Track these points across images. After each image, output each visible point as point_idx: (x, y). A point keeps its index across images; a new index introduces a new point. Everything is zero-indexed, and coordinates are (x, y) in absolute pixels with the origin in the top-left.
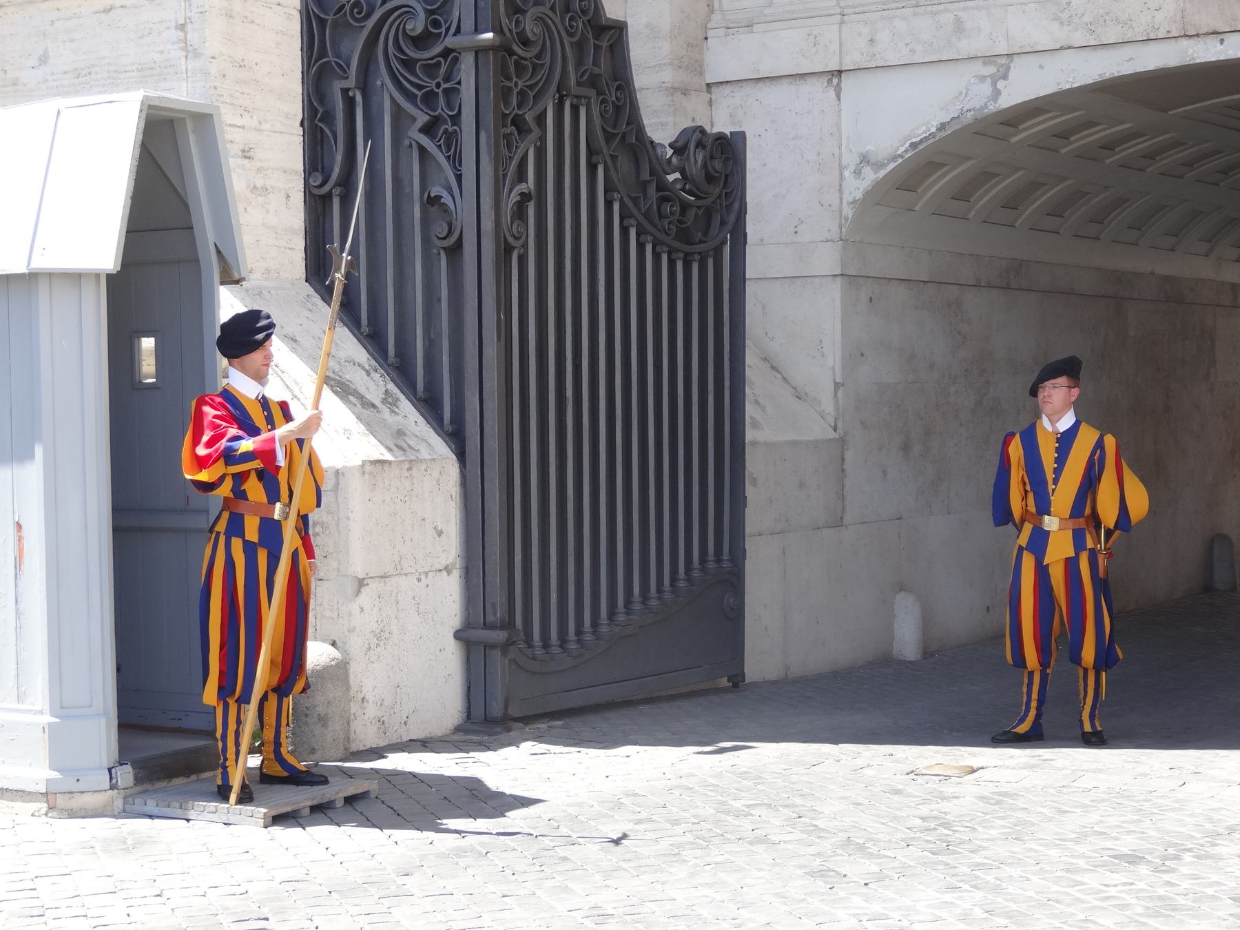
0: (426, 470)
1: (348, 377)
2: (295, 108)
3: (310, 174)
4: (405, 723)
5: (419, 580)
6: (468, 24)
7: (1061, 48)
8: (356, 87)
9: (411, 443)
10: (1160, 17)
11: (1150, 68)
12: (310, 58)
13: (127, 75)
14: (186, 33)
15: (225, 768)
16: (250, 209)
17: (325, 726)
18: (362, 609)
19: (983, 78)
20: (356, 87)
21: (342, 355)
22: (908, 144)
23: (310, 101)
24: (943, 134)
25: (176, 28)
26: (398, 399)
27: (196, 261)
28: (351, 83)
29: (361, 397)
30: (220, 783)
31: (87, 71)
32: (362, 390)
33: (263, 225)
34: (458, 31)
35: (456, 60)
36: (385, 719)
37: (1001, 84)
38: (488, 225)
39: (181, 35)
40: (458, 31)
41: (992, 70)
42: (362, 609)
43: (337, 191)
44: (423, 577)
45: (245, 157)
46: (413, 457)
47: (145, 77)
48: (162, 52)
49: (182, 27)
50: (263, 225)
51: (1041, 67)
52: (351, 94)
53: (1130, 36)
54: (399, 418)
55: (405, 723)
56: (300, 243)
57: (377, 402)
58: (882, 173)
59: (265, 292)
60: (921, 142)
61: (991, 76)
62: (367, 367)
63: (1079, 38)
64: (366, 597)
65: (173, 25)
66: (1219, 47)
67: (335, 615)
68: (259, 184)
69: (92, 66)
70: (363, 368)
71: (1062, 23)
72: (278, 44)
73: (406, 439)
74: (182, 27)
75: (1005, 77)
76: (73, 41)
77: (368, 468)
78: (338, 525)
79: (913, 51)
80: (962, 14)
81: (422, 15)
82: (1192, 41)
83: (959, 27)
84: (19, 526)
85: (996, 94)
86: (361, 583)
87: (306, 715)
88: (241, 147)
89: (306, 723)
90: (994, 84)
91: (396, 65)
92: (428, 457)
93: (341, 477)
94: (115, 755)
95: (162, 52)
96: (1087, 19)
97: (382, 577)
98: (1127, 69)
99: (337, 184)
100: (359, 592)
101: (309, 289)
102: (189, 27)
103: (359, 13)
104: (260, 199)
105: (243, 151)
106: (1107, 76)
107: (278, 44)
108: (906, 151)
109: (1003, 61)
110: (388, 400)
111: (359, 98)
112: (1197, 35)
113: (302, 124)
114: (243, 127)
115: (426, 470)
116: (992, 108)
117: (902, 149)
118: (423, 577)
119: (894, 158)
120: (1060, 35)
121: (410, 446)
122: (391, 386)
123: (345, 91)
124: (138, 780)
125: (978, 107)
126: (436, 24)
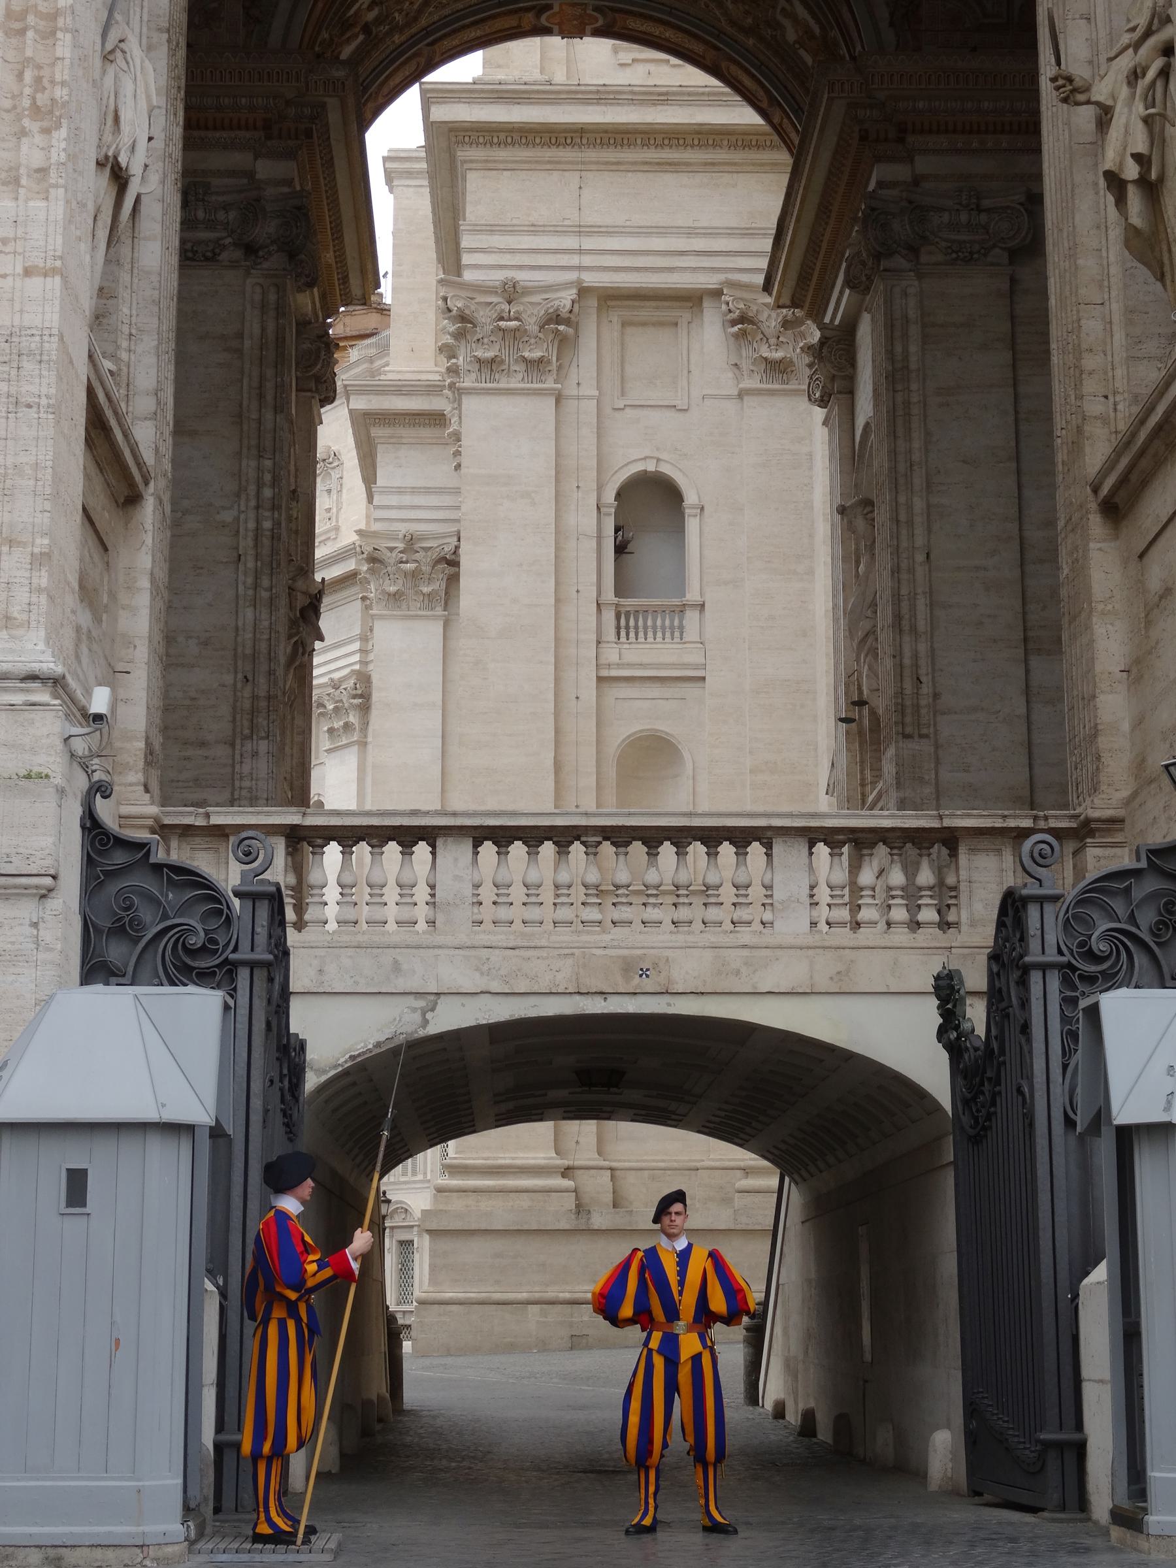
6: (245, 944)
7: (482, 992)
10: (560, 976)
11: (550, 1014)
19: (414, 1010)
22: (347, 1056)
24: (379, 1051)
25: (31, 925)
34: (235, 950)
35: (230, 972)
37: (429, 1016)
38: (257, 1103)
39: (35, 932)
40: (235, 950)
41: (421, 1003)
48: (13, 943)
49: (35, 925)
51: (463, 1005)
53: (536, 989)
58: (324, 1078)
60: (359, 1055)
61: (422, 1009)
63: (496, 986)
65: (27, 922)
66: (603, 1003)
71: (482, 974)
74: (35, 925)
75: (433, 1010)
79: (356, 983)
80: (399, 958)
81: (202, 934)
82: (582, 997)
83: (397, 967)
85: (425, 1023)
90: (424, 1014)
91: (172, 970)
96: (503, 972)
98: (533, 1013)
102: (41, 925)
106: (517, 1017)
108: (346, 1062)
109: (432, 998)
112: (588, 993)
116: (422, 1033)
117: (342, 1060)
119: (336, 1067)
120: (480, 983)
125: (409, 1030)
126: (213, 941)
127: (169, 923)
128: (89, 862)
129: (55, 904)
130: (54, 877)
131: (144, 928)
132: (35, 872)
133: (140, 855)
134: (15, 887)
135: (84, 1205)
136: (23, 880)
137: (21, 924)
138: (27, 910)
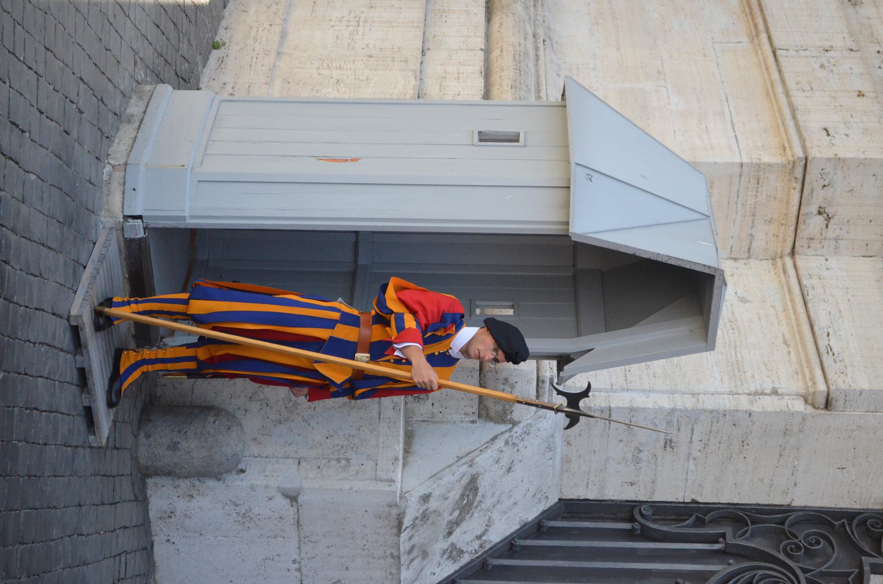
0: (391, 573)
1: (476, 515)
2: (707, 496)
3: (652, 507)
4: (168, 541)
5: (294, 561)
8: (726, 544)
9: (416, 562)
12: (750, 510)
13: (733, 353)
14: (770, 395)
15: (129, 303)
16: (621, 445)
17: (169, 448)
18: (270, 499)
20: (726, 544)
21: (495, 515)
23: (713, 510)
25: (773, 388)
26: (455, 561)
27: (579, 334)
28: (730, 540)
29: (457, 523)
30: (115, 300)
31: (735, 327)
32: (464, 526)
33: (608, 458)
36: (173, 519)
39: (769, 391)
42: (270, 499)
43: (637, 526)
44: (296, 566)
45: (666, 443)
46: (402, 560)
47: (733, 365)
48: (753, 377)
50: (608, 458)
52: (721, 540)
54: (438, 558)
55: (168, 541)
56: (592, 494)
57: (453, 539)
59: (550, 454)
62: (484, 538)
64: (282, 503)
65: (777, 386)
67: (267, 473)
68: (644, 456)
69: (739, 330)
70: (483, 534)
72: (762, 481)
73: (420, 559)
76: (759, 319)
77: (395, 511)
78: (345, 479)
84: (354, 160)
86: (293, 498)
87: (180, 432)
88: (674, 439)
89: (173, 431)
91: (747, 575)
92: (402, 578)
93: (387, 484)
94: (153, 224)
95: (753, 377)
97: (298, 522)
99: (642, 525)
100: (286, 496)
101: (553, 500)
102: (776, 398)
103: (791, 549)
104: (629, 456)
105: (671, 441)
107: (762, 481)
110: (454, 552)
111: (716, 547)
113: (694, 502)
114: (691, 442)
115: (391, 573)
118: (296, 566)
121: (412, 560)
122: (466, 559)
123: (723, 535)
124: (129, 242)
127: (799, 572)
128: (850, 515)
129: (799, 406)
130: (828, 405)
131: (788, 555)
132: (829, 377)
133: (867, 549)
134: (812, 372)
135: (481, 140)
136: (818, 373)
137: (773, 382)
138: (790, 384)
